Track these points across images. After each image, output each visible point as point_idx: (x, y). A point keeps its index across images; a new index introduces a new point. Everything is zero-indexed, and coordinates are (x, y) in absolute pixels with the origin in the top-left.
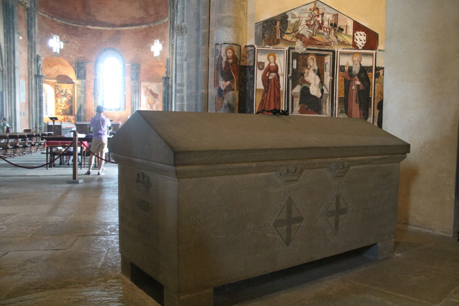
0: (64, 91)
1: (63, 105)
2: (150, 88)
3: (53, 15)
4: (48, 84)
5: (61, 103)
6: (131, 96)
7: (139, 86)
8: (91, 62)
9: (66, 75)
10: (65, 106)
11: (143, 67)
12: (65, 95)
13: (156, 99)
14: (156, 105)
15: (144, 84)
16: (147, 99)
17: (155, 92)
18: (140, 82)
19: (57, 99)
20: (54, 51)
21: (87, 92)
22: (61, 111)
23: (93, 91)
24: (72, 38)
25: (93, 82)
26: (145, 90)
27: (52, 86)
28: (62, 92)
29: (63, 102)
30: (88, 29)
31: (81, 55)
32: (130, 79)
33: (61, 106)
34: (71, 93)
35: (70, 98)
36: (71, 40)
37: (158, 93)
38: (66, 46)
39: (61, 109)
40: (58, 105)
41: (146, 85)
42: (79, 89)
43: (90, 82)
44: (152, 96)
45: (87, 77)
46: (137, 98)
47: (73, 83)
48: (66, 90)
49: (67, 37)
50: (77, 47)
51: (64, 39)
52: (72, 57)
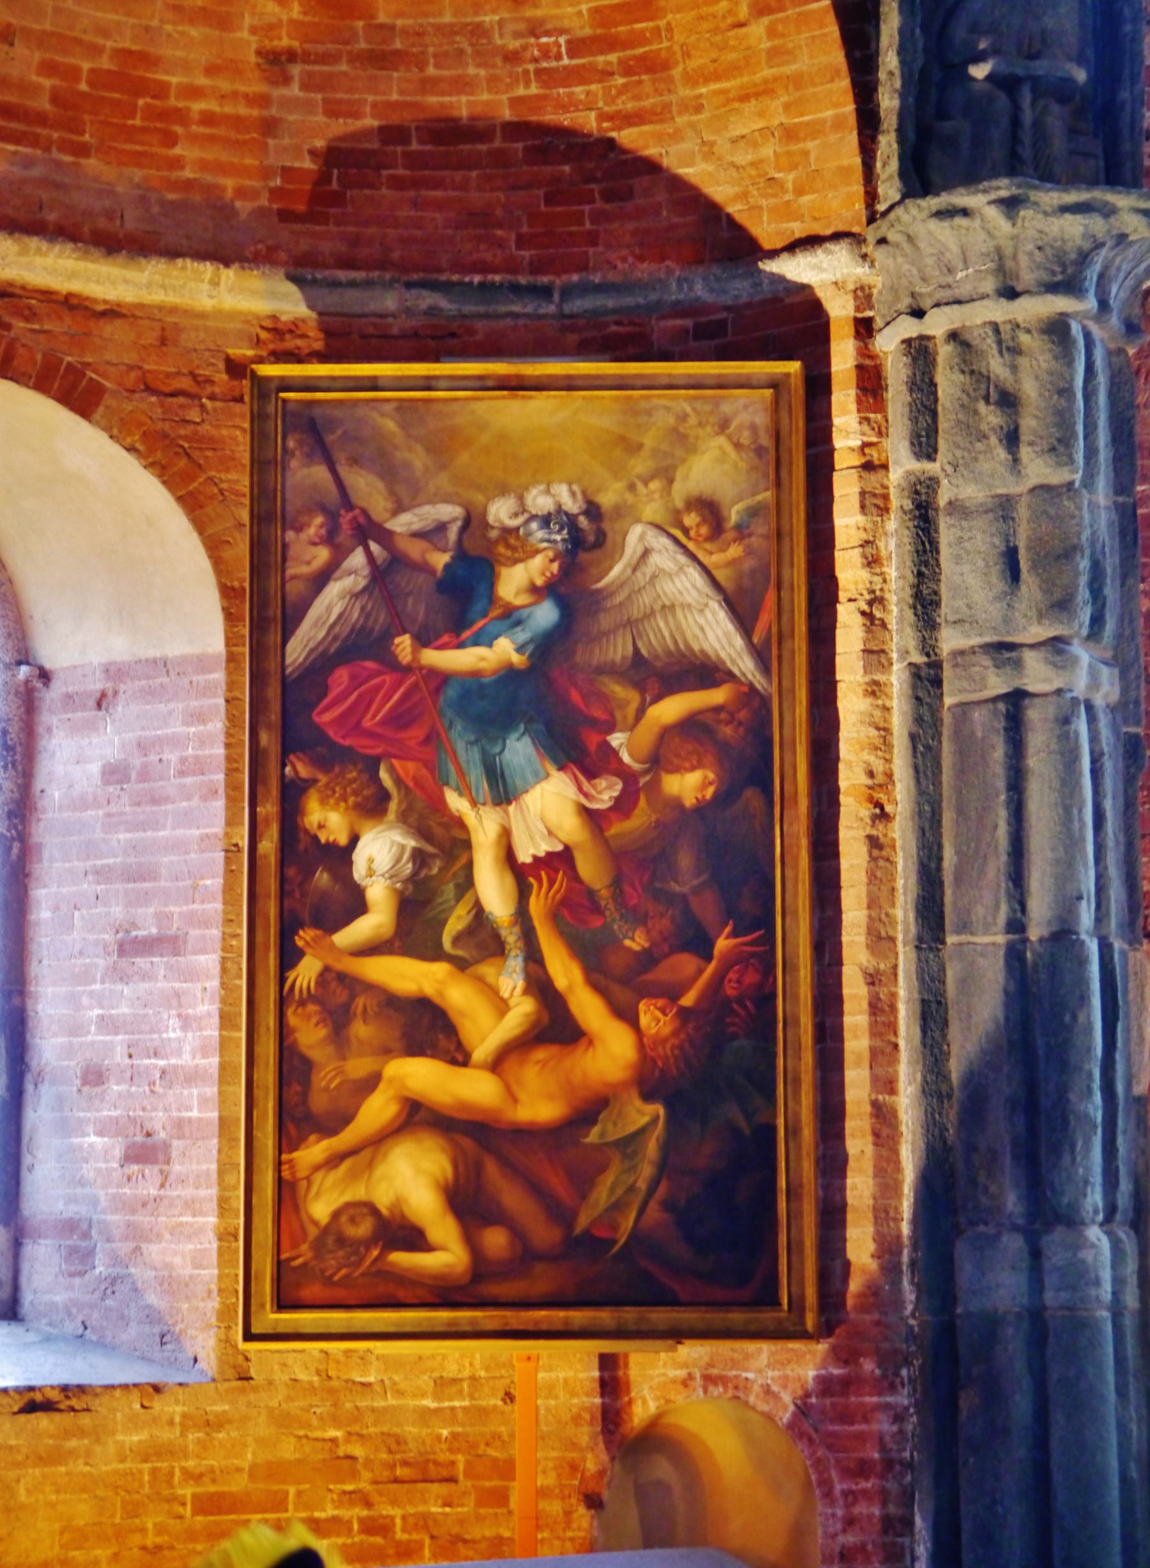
0: (513, 582)
1: (491, 1009)
4: (78, 394)
5: (414, 930)
9: (585, 111)
10: (555, 1027)
12: (554, 708)
19: (327, 819)
22: (412, 1179)
27: (175, 460)
28: (464, 593)
29: (493, 891)
33: (428, 1029)
34: (716, 633)
35: (688, 785)
39: (416, 1116)
40: (341, 995)
42: (970, 480)
47: (796, 325)
48: (585, 539)
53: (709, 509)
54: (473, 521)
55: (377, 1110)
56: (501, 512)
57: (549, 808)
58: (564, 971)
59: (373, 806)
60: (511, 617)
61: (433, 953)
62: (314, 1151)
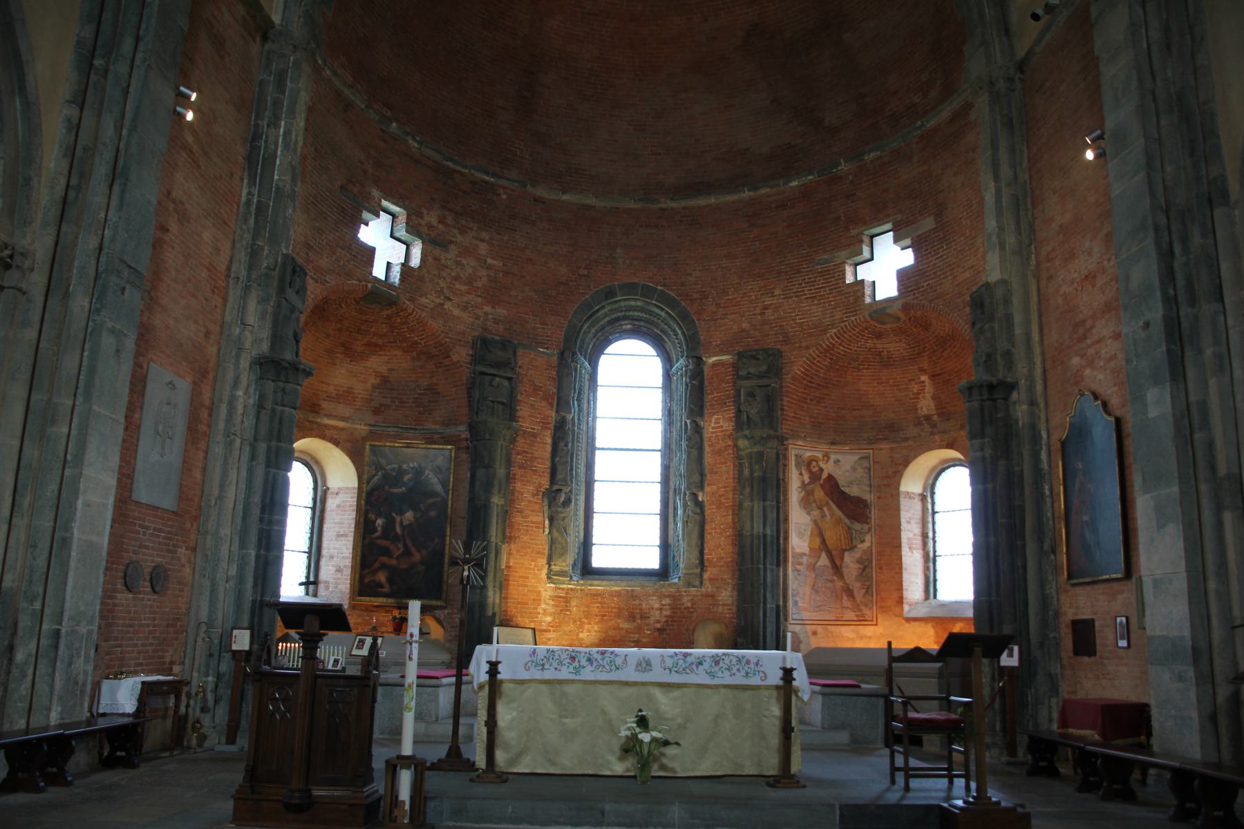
0: (406, 478)
1: (398, 550)
2: (828, 468)
3: (389, 114)
6: (738, 508)
7: (780, 459)
8: (541, 344)
10: (407, 553)
11: (796, 365)
13: (857, 526)
14: (858, 555)
15: (798, 450)
16: (815, 522)
17: (854, 491)
18: (782, 440)
20: (379, 271)
21: (518, 485)
22: (382, 577)
23: (545, 482)
24: (463, 231)
25: (549, 440)
26: (806, 478)
29: (398, 530)
30: (537, 200)
31: (501, 312)
32: (728, 426)
33: (387, 552)
34: (439, 488)
35: (433, 513)
36: (459, 238)
37: (868, 497)
38: (436, 259)
39: (383, 566)
41: (808, 454)
43: (534, 436)
44: (838, 513)
45: (523, 411)
46: (772, 516)
49: (442, 220)
50: (484, 273)
51: (430, 227)
52: (456, 312)
53: (439, 468)
54: (400, 467)
55: (377, 565)
56: (405, 466)
57: (409, 516)
58: (409, 544)
59: (379, 515)
60: (404, 484)
61: (387, 539)
62: (366, 571)
